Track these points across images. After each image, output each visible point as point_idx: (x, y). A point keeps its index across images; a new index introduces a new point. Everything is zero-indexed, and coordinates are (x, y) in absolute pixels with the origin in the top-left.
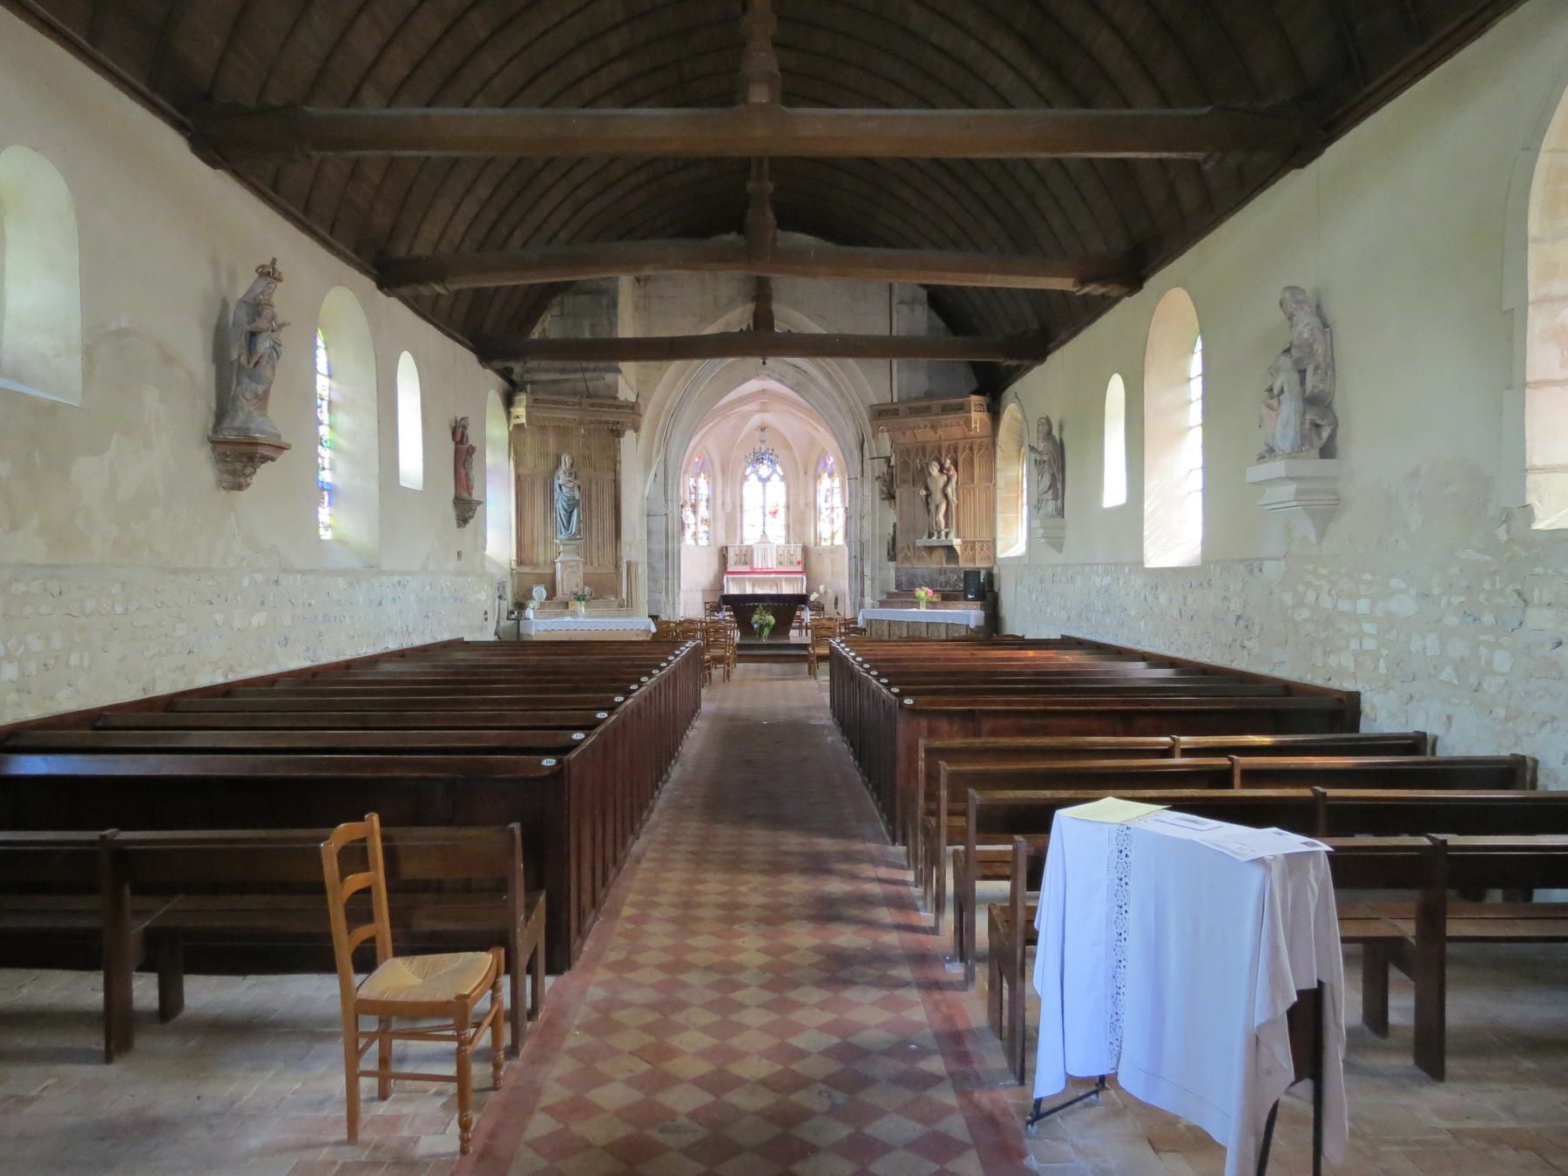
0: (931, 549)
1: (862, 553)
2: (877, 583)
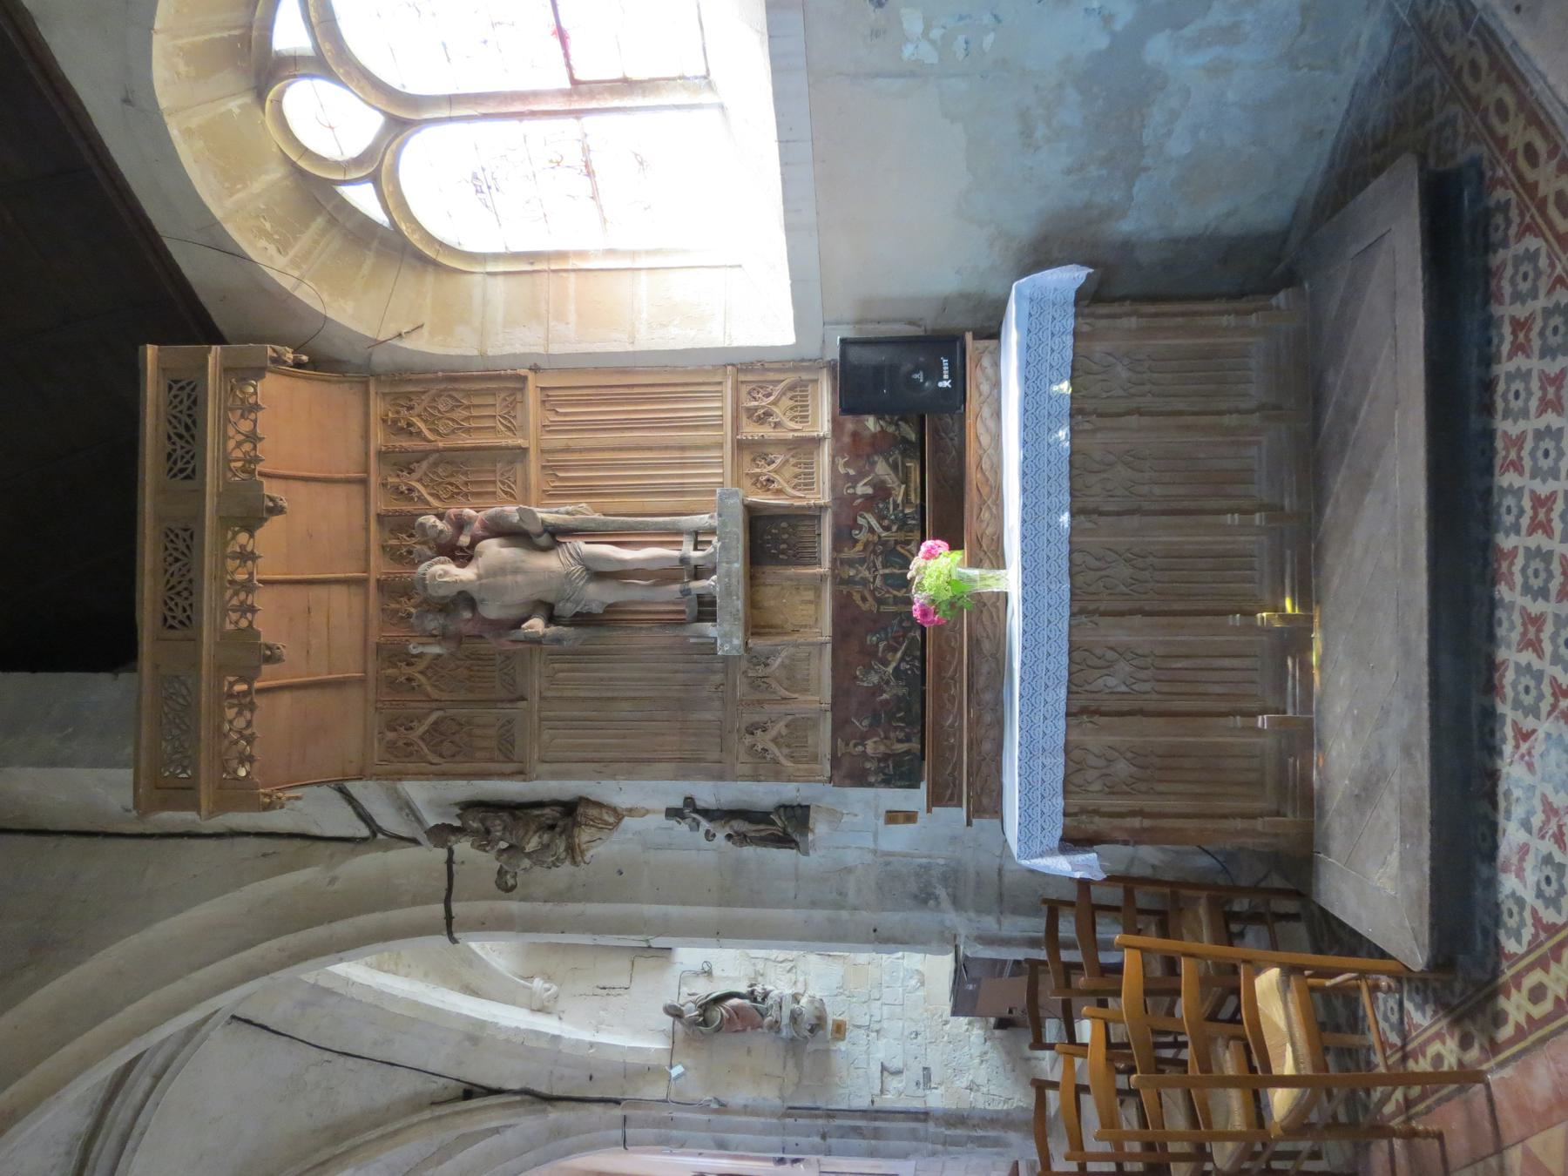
0: (756, 626)
1: (812, 1112)
2: (892, 919)
